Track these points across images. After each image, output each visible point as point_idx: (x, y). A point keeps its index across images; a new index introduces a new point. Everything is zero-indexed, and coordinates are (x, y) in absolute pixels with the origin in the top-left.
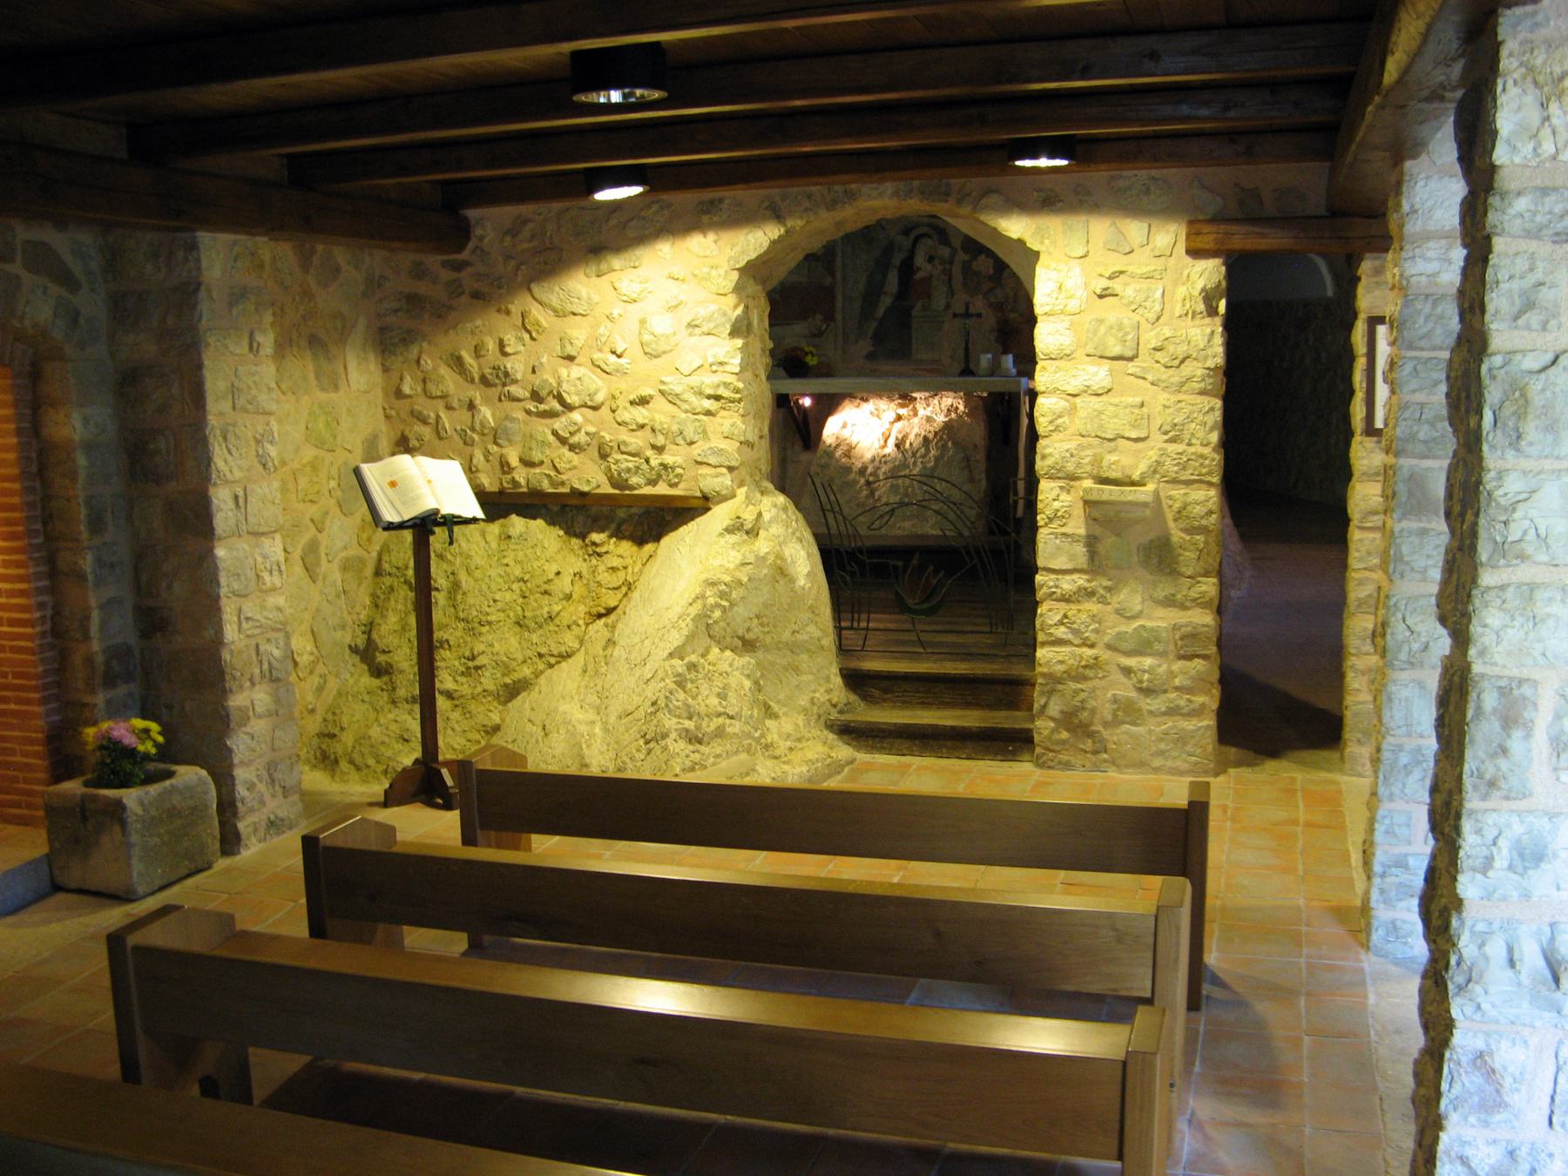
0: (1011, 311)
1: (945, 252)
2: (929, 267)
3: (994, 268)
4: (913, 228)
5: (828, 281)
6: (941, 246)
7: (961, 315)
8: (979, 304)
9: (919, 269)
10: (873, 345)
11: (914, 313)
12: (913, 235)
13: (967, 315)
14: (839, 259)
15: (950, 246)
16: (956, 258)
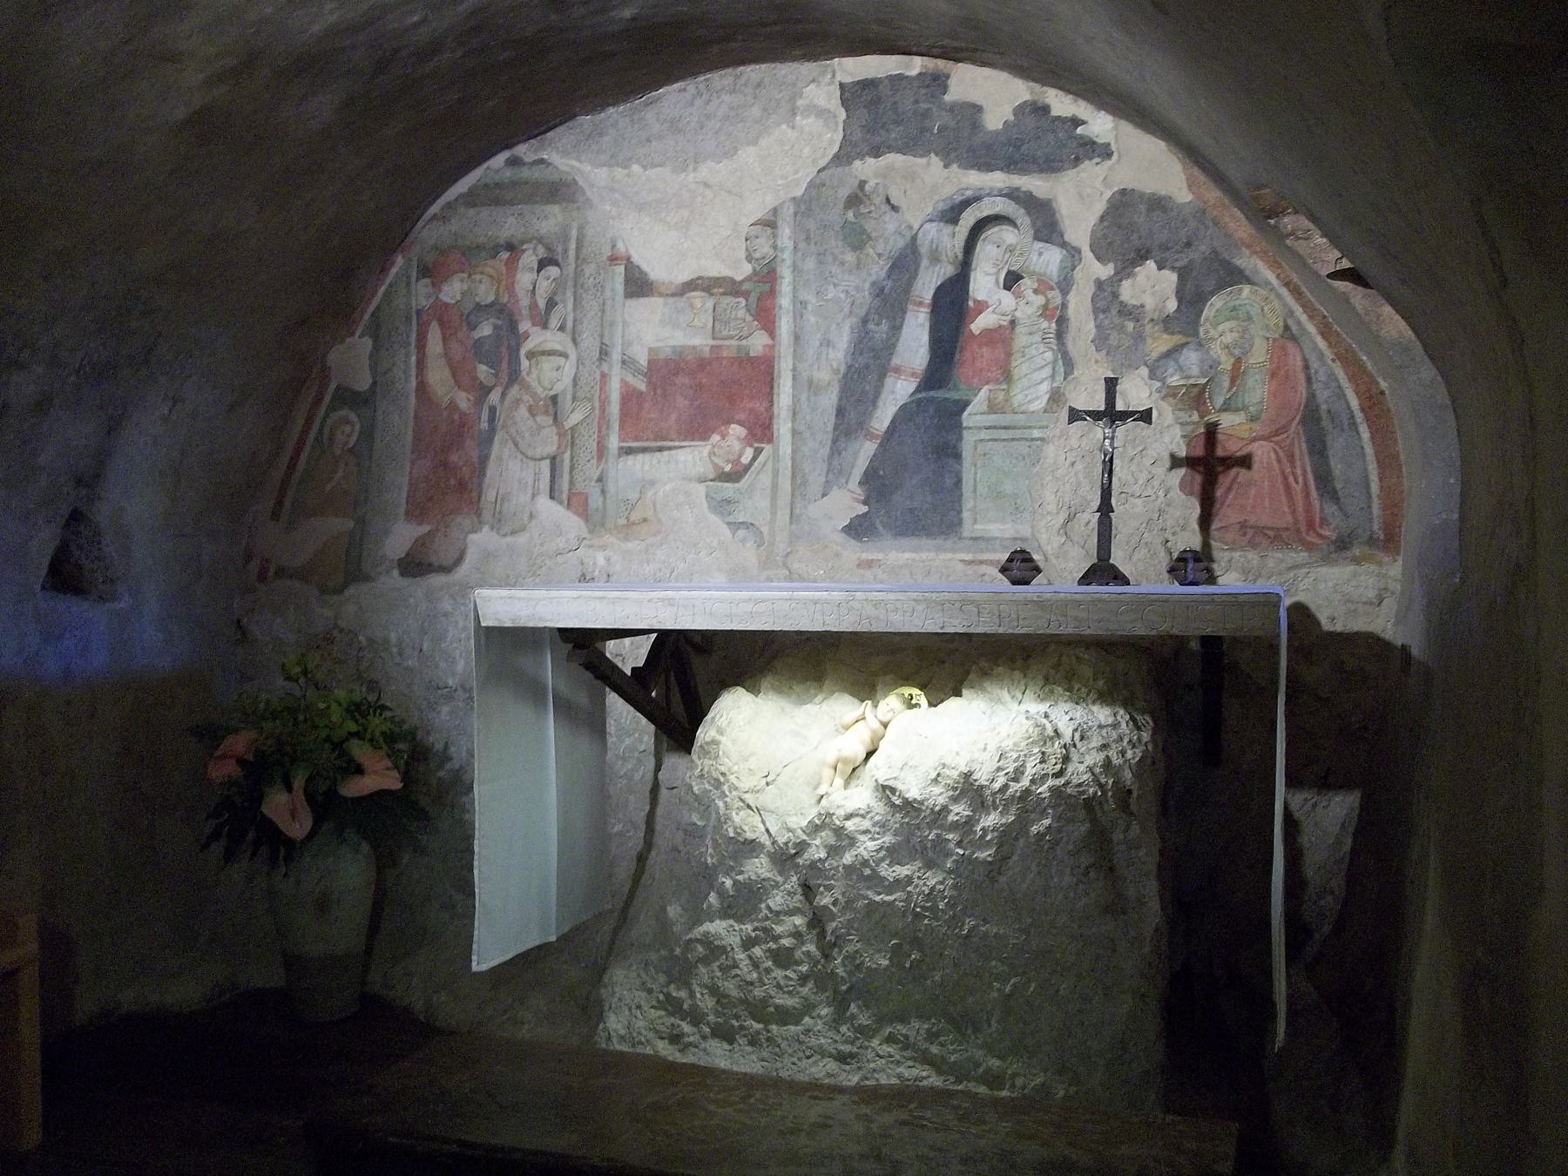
0: (1226, 408)
1: (1049, 259)
2: (1007, 299)
3: (1180, 294)
4: (967, 203)
5: (758, 343)
6: (1039, 245)
7: (1096, 416)
8: (1136, 392)
9: (981, 307)
10: (865, 503)
11: (968, 418)
12: (969, 218)
13: (1111, 415)
14: (785, 287)
15: (1064, 245)
16: (1078, 273)
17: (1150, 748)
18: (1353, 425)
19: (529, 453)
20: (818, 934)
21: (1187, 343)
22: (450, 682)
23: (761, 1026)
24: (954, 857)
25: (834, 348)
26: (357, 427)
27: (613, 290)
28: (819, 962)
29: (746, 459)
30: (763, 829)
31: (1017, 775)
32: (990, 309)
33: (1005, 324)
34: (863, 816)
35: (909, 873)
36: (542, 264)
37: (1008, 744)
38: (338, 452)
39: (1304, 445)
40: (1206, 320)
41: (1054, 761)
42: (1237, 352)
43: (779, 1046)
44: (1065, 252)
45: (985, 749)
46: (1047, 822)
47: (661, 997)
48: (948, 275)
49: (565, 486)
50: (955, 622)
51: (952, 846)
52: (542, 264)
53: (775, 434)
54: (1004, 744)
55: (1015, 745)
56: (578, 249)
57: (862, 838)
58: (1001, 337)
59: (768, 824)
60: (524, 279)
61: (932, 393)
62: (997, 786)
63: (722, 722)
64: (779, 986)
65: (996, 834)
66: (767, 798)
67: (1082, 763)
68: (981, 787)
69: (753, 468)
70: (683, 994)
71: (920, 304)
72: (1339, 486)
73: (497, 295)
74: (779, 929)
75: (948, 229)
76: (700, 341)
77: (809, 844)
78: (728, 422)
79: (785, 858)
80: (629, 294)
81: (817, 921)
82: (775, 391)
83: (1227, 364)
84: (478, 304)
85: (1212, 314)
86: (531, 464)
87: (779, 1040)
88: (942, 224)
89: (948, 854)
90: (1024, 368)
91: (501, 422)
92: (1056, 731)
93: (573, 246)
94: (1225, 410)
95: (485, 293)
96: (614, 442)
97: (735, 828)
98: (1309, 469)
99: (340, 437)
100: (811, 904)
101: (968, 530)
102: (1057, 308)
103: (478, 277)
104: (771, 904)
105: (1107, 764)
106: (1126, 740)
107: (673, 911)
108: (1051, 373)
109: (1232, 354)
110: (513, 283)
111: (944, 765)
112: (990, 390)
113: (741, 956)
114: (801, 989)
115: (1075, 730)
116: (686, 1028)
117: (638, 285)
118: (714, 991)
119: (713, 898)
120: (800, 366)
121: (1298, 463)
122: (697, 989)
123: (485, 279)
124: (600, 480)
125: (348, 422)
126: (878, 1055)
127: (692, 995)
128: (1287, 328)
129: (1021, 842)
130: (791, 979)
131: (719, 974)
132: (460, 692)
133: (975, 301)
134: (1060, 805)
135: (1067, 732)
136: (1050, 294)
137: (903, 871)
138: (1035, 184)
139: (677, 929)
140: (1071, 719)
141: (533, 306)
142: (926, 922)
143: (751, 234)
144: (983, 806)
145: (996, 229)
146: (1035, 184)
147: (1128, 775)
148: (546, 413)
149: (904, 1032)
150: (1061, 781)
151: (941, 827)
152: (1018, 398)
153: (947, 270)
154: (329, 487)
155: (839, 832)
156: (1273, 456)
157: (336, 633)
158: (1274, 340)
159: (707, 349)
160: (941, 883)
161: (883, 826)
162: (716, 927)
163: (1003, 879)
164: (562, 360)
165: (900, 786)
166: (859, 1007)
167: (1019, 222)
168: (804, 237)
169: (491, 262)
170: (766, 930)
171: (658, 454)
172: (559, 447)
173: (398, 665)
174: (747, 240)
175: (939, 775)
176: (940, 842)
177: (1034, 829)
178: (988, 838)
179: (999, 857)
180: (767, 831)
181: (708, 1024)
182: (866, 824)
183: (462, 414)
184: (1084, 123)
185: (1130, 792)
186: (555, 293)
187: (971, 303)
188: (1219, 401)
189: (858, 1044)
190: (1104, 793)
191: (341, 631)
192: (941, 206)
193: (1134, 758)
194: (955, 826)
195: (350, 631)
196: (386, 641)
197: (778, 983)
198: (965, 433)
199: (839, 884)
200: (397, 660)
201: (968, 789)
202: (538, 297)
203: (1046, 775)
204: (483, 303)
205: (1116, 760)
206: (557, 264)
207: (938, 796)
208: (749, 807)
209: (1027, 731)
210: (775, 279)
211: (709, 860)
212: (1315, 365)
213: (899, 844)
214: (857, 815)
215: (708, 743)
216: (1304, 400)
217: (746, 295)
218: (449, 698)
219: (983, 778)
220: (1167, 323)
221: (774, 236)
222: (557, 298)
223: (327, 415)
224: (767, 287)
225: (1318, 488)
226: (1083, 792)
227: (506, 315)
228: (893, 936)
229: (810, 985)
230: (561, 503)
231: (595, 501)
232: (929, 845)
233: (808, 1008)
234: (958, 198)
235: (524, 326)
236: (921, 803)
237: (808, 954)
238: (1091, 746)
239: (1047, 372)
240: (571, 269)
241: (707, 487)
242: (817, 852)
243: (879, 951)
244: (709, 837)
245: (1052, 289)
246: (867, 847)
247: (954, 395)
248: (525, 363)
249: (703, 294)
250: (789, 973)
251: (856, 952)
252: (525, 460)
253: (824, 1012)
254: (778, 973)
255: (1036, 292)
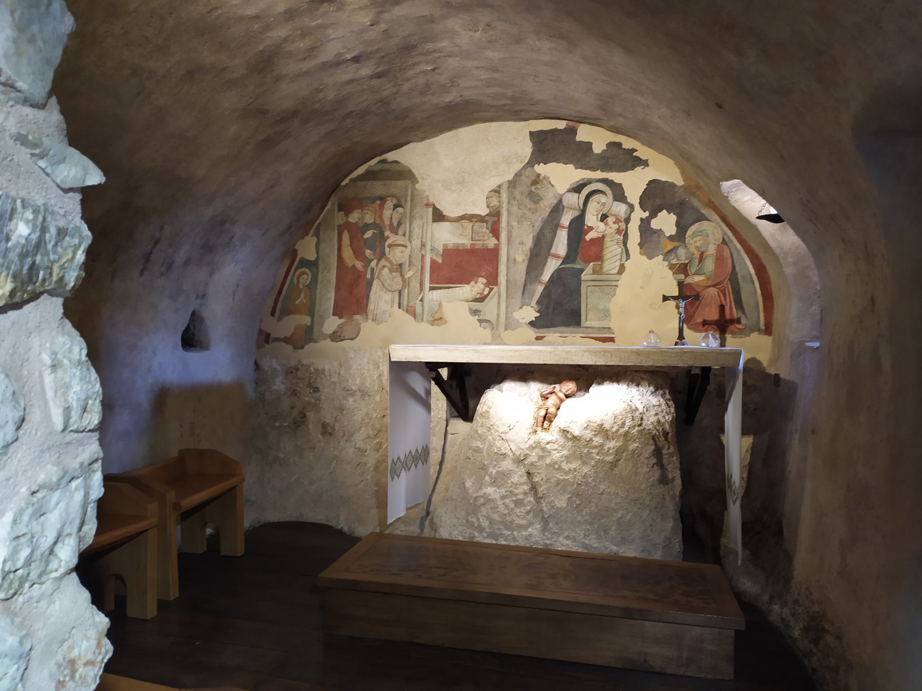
0: (696, 273)
1: (620, 209)
2: (602, 226)
3: (678, 225)
5: (491, 242)
6: (616, 203)
9: (591, 229)
10: (538, 312)
11: (584, 276)
17: (674, 415)
18: (753, 282)
19: (389, 289)
20: (534, 493)
21: (679, 246)
22: (354, 388)
23: (510, 533)
24: (596, 460)
25: (525, 245)
26: (310, 277)
27: (427, 218)
28: (535, 505)
29: (486, 293)
30: (509, 449)
31: (623, 424)
32: (594, 230)
33: (601, 236)
34: (554, 443)
35: (575, 467)
36: (396, 206)
37: (617, 412)
38: (301, 287)
39: (730, 290)
40: (689, 236)
41: (637, 420)
42: (702, 250)
43: (518, 541)
44: (627, 206)
45: (607, 415)
46: (636, 445)
47: (464, 521)
48: (576, 215)
49: (406, 303)
50: (601, 360)
51: (594, 455)
52: (396, 206)
53: (499, 282)
54: (615, 413)
55: (620, 413)
56: (412, 200)
57: (554, 452)
58: (600, 241)
59: (511, 447)
60: (387, 213)
61: (568, 266)
62: (614, 430)
63: (489, 404)
64: (518, 516)
65: (614, 450)
66: (510, 436)
67: (648, 421)
68: (607, 430)
69: (489, 296)
70: (474, 520)
71: (564, 228)
72: (745, 306)
73: (375, 219)
74: (517, 491)
75: (576, 195)
76: (466, 242)
77: (530, 455)
78: (479, 276)
79: (519, 461)
80: (434, 221)
81: (534, 488)
82: (499, 264)
83: (697, 255)
84: (366, 223)
85: (691, 233)
86: (390, 293)
87: (518, 539)
88: (574, 193)
89: (593, 459)
90: (608, 256)
91: (376, 275)
92: (636, 407)
93: (409, 199)
94: (696, 274)
95: (369, 218)
96: (427, 285)
97: (497, 448)
98: (732, 299)
99: (302, 280)
100: (531, 481)
101: (583, 324)
102: (623, 230)
103: (366, 211)
104: (513, 480)
105: (659, 422)
106: (665, 412)
107: (468, 484)
108: (620, 257)
109: (700, 251)
110: (382, 214)
111: (590, 421)
112: (594, 265)
113: (500, 503)
114: (527, 517)
115: (644, 407)
116: (476, 534)
117: (439, 216)
118: (488, 518)
119: (487, 478)
120: (511, 252)
121: (728, 297)
122: (480, 517)
123: (369, 212)
124: (421, 300)
125: (305, 273)
126: (562, 545)
127: (478, 520)
128: (723, 239)
129: (625, 454)
130: (522, 512)
131: (490, 511)
132: (358, 392)
133: (588, 226)
134: (642, 438)
135: (641, 408)
136: (620, 224)
137: (572, 466)
138: (615, 177)
139: (471, 491)
140: (641, 403)
141: (391, 224)
142: (583, 487)
143: (489, 195)
144: (608, 439)
145: (598, 195)
146: (615, 177)
147: (667, 427)
148: (397, 272)
149: (573, 534)
150: (642, 428)
151: (590, 448)
152: (605, 270)
153: (577, 213)
154: (297, 302)
155: (543, 449)
156: (716, 293)
157: (299, 366)
158: (718, 245)
159: (469, 245)
160: (590, 471)
161: (563, 447)
162: (489, 490)
163: (616, 469)
164: (405, 248)
165: (571, 430)
166: (553, 524)
167: (607, 193)
168: (511, 197)
169: (372, 205)
170: (511, 492)
171: (447, 290)
172: (403, 286)
173: (329, 380)
174: (487, 198)
175: (588, 425)
176: (589, 453)
177: (631, 448)
178: (611, 452)
179: (615, 460)
180: (511, 449)
181: (486, 532)
182: (556, 446)
183: (359, 271)
184: (636, 151)
185: (668, 433)
186: (401, 219)
187: (586, 227)
188: (693, 271)
189: (553, 540)
190: (659, 433)
191: (302, 365)
192: (575, 186)
193: (669, 419)
194: (595, 447)
195: (307, 365)
196: (323, 370)
197: (517, 515)
198: (582, 282)
199: (544, 472)
200: (328, 378)
201: (601, 430)
202: (393, 221)
203: (635, 425)
204: (368, 223)
205: (662, 420)
206: (401, 206)
207: (588, 434)
208: (503, 439)
209: (625, 407)
210: (500, 216)
211: (486, 463)
212: (735, 256)
213: (570, 455)
214: (552, 442)
215: (484, 412)
216: (730, 270)
217: (486, 222)
218: (352, 395)
219: (608, 426)
220: (671, 238)
221: (499, 197)
222: (402, 222)
223: (295, 271)
224: (496, 219)
225: (736, 308)
226: (651, 433)
227: (379, 228)
228: (568, 494)
229: (531, 515)
230: (403, 310)
231: (418, 310)
232: (584, 455)
233: (530, 524)
234: (582, 182)
235: (387, 233)
236: (580, 437)
237: (530, 502)
238: (651, 414)
239: (619, 257)
240: (408, 211)
241: (469, 304)
242: (533, 458)
243: (562, 500)
244: (485, 452)
245: (622, 222)
246: (556, 456)
247: (578, 266)
248: (387, 250)
249: (468, 221)
250: (522, 510)
251: (552, 501)
252: (387, 291)
253: (538, 526)
254: (517, 510)
255: (614, 223)
